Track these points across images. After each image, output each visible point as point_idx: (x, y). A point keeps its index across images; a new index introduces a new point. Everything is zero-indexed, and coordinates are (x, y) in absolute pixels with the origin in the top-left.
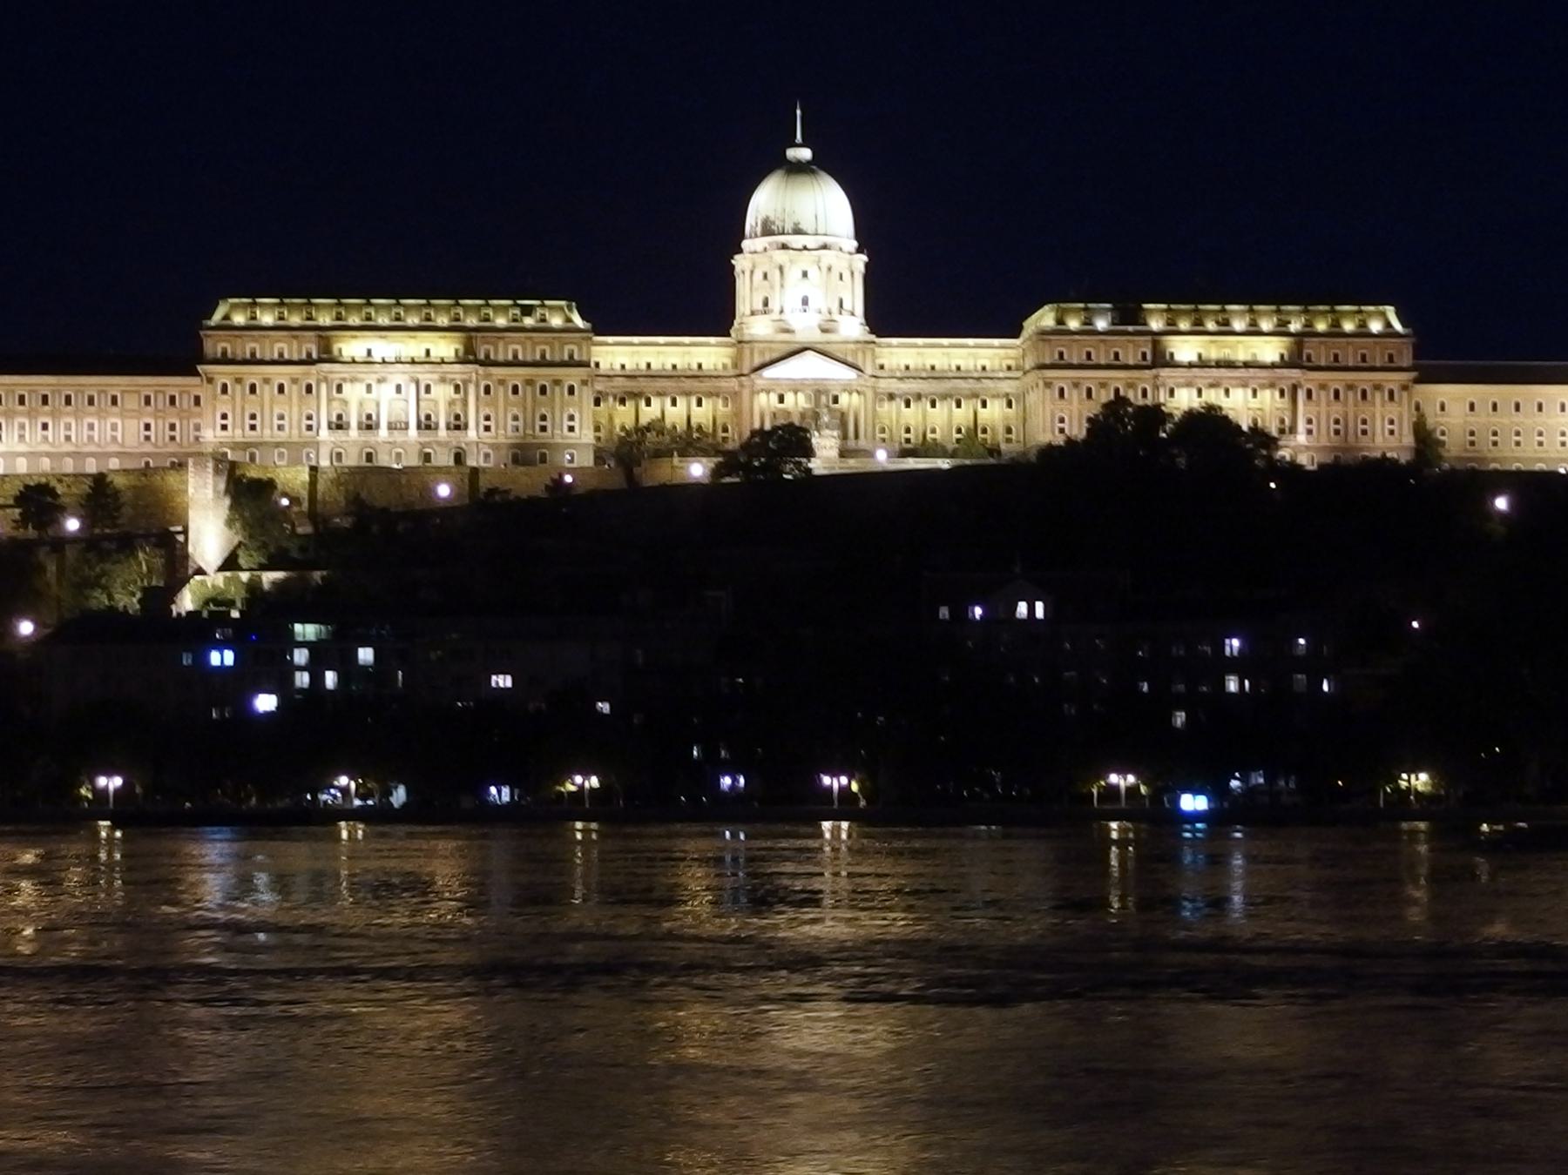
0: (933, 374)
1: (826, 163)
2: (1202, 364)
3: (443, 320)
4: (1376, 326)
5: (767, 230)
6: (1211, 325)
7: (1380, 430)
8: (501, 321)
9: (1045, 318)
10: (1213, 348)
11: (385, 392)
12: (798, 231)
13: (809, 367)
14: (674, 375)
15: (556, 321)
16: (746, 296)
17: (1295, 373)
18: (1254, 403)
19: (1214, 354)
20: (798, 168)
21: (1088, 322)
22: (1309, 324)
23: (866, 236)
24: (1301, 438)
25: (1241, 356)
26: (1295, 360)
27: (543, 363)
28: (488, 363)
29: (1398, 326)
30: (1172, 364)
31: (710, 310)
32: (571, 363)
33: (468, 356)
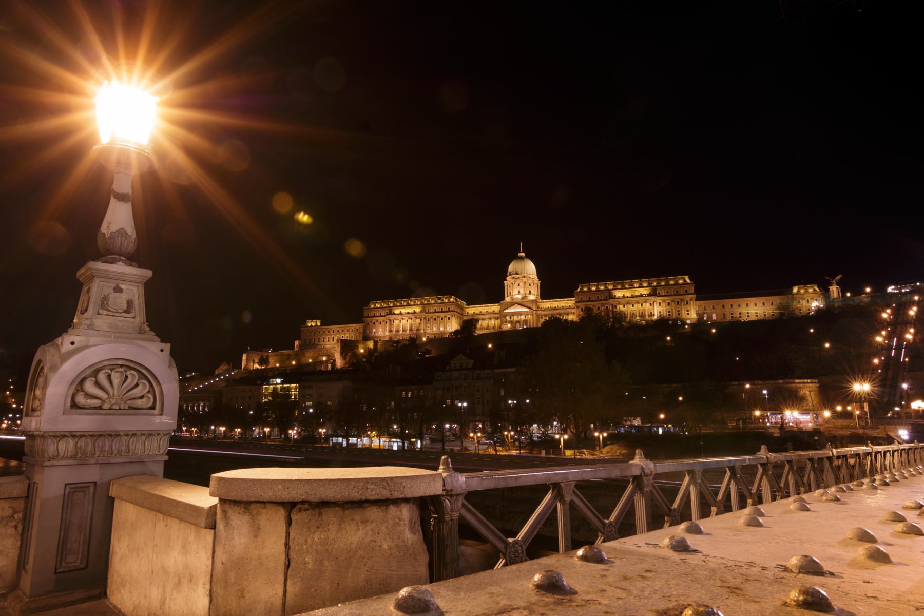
1: (529, 256)
2: (624, 297)
6: (627, 286)
10: (628, 293)
11: (404, 322)
12: (517, 273)
14: (487, 313)
17: (653, 297)
18: (641, 308)
20: (521, 258)
25: (637, 294)
29: (688, 281)
30: (615, 297)
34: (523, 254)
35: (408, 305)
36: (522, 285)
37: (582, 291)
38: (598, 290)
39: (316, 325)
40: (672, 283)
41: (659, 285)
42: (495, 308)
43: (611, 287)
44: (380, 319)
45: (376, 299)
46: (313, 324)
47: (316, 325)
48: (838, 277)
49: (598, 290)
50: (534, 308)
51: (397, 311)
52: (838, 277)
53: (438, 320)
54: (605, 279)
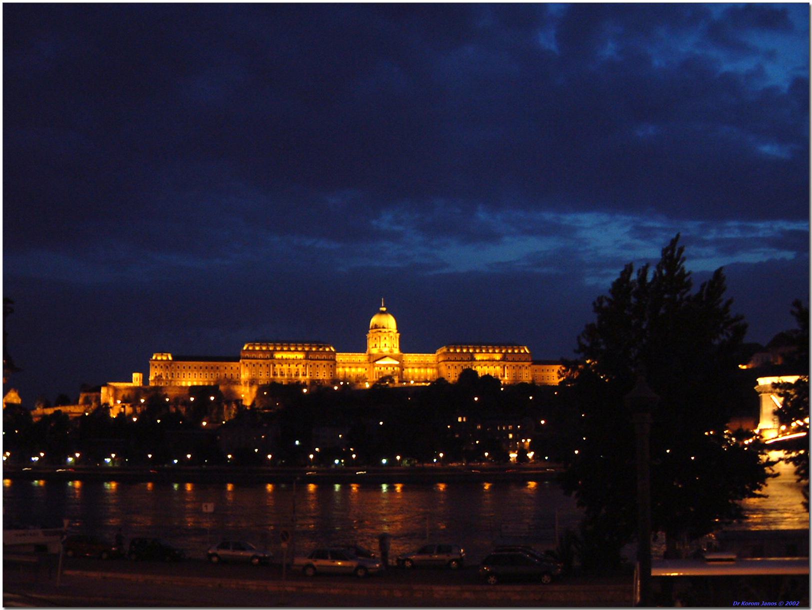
3: (300, 349)
4: (522, 351)
7: (524, 375)
8: (314, 349)
9: (445, 350)
12: (384, 328)
16: (371, 344)
17: (504, 363)
20: (383, 313)
24: (506, 378)
26: (504, 359)
27: (324, 360)
28: (311, 359)
30: (475, 360)
31: (361, 347)
32: (331, 360)
33: (306, 358)
34: (384, 309)
35: (289, 350)
38: (462, 352)
39: (168, 360)
41: (507, 353)
42: (361, 357)
43: (471, 351)
44: (261, 361)
46: (165, 358)
47: (168, 360)
49: (462, 352)
51: (278, 356)
53: (321, 367)
54: (467, 344)
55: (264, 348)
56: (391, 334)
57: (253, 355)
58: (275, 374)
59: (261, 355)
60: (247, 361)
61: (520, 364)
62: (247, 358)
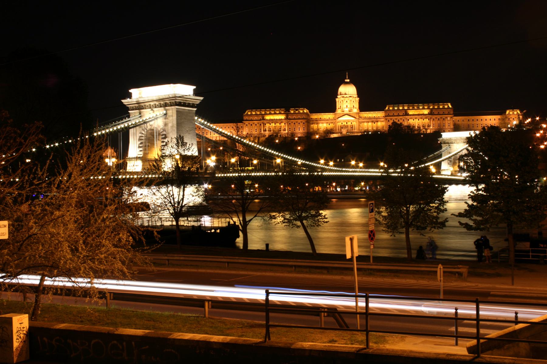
0: (370, 118)
1: (352, 82)
2: (414, 115)
5: (341, 94)
6: (416, 108)
10: (416, 112)
12: (345, 94)
13: (346, 118)
15: (301, 112)
18: (424, 121)
19: (416, 113)
20: (347, 83)
21: (393, 108)
22: (434, 107)
23: (359, 94)
25: (421, 113)
26: (431, 113)
28: (290, 119)
30: (408, 115)
33: (287, 118)
34: (348, 80)
35: (275, 114)
36: (348, 101)
37: (389, 110)
38: (398, 110)
40: (441, 107)
41: (434, 108)
43: (406, 108)
44: (256, 122)
45: (252, 108)
48: (525, 111)
50: (357, 117)
51: (268, 117)
52: (525, 111)
54: (403, 103)
55: (258, 113)
56: (351, 98)
57: (251, 118)
58: (265, 131)
59: (256, 118)
60: (247, 123)
61: (444, 116)
62: (247, 120)
